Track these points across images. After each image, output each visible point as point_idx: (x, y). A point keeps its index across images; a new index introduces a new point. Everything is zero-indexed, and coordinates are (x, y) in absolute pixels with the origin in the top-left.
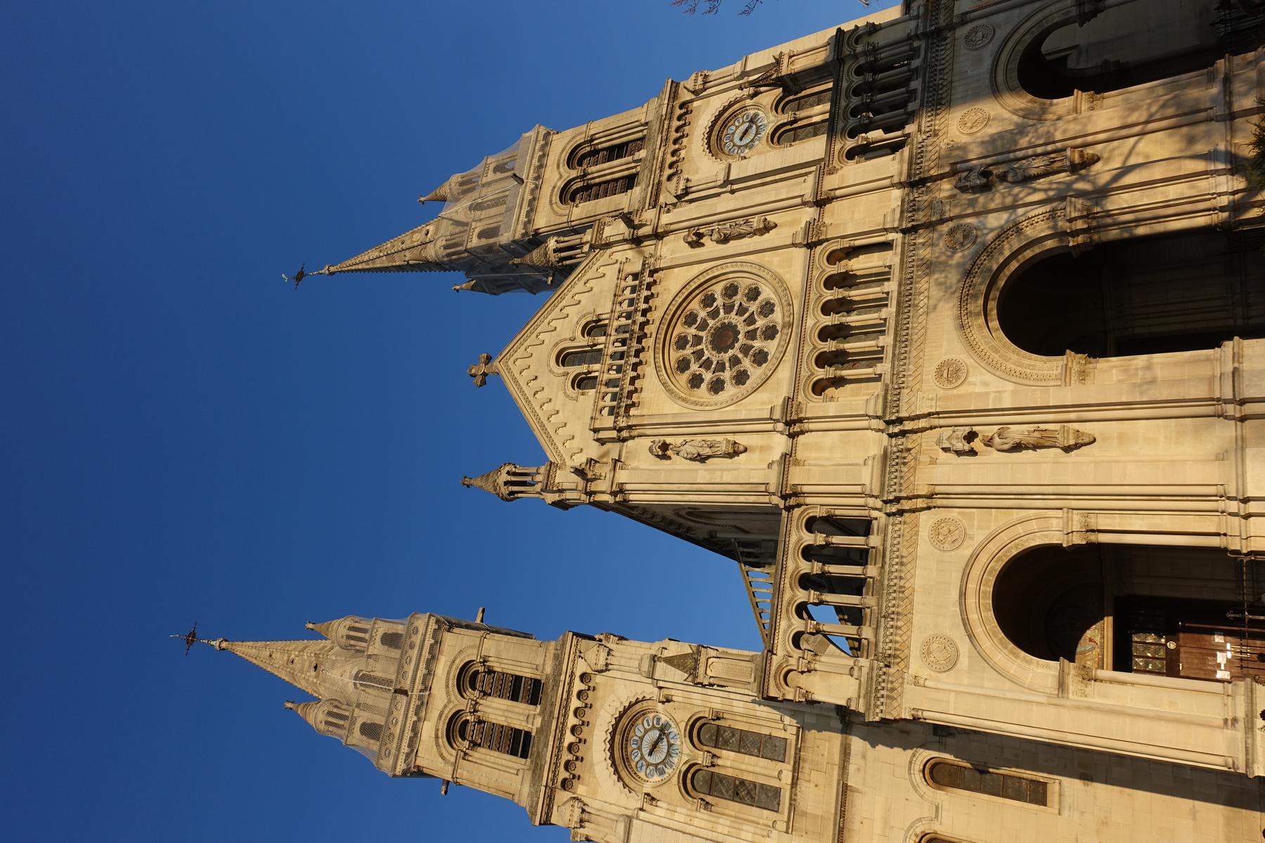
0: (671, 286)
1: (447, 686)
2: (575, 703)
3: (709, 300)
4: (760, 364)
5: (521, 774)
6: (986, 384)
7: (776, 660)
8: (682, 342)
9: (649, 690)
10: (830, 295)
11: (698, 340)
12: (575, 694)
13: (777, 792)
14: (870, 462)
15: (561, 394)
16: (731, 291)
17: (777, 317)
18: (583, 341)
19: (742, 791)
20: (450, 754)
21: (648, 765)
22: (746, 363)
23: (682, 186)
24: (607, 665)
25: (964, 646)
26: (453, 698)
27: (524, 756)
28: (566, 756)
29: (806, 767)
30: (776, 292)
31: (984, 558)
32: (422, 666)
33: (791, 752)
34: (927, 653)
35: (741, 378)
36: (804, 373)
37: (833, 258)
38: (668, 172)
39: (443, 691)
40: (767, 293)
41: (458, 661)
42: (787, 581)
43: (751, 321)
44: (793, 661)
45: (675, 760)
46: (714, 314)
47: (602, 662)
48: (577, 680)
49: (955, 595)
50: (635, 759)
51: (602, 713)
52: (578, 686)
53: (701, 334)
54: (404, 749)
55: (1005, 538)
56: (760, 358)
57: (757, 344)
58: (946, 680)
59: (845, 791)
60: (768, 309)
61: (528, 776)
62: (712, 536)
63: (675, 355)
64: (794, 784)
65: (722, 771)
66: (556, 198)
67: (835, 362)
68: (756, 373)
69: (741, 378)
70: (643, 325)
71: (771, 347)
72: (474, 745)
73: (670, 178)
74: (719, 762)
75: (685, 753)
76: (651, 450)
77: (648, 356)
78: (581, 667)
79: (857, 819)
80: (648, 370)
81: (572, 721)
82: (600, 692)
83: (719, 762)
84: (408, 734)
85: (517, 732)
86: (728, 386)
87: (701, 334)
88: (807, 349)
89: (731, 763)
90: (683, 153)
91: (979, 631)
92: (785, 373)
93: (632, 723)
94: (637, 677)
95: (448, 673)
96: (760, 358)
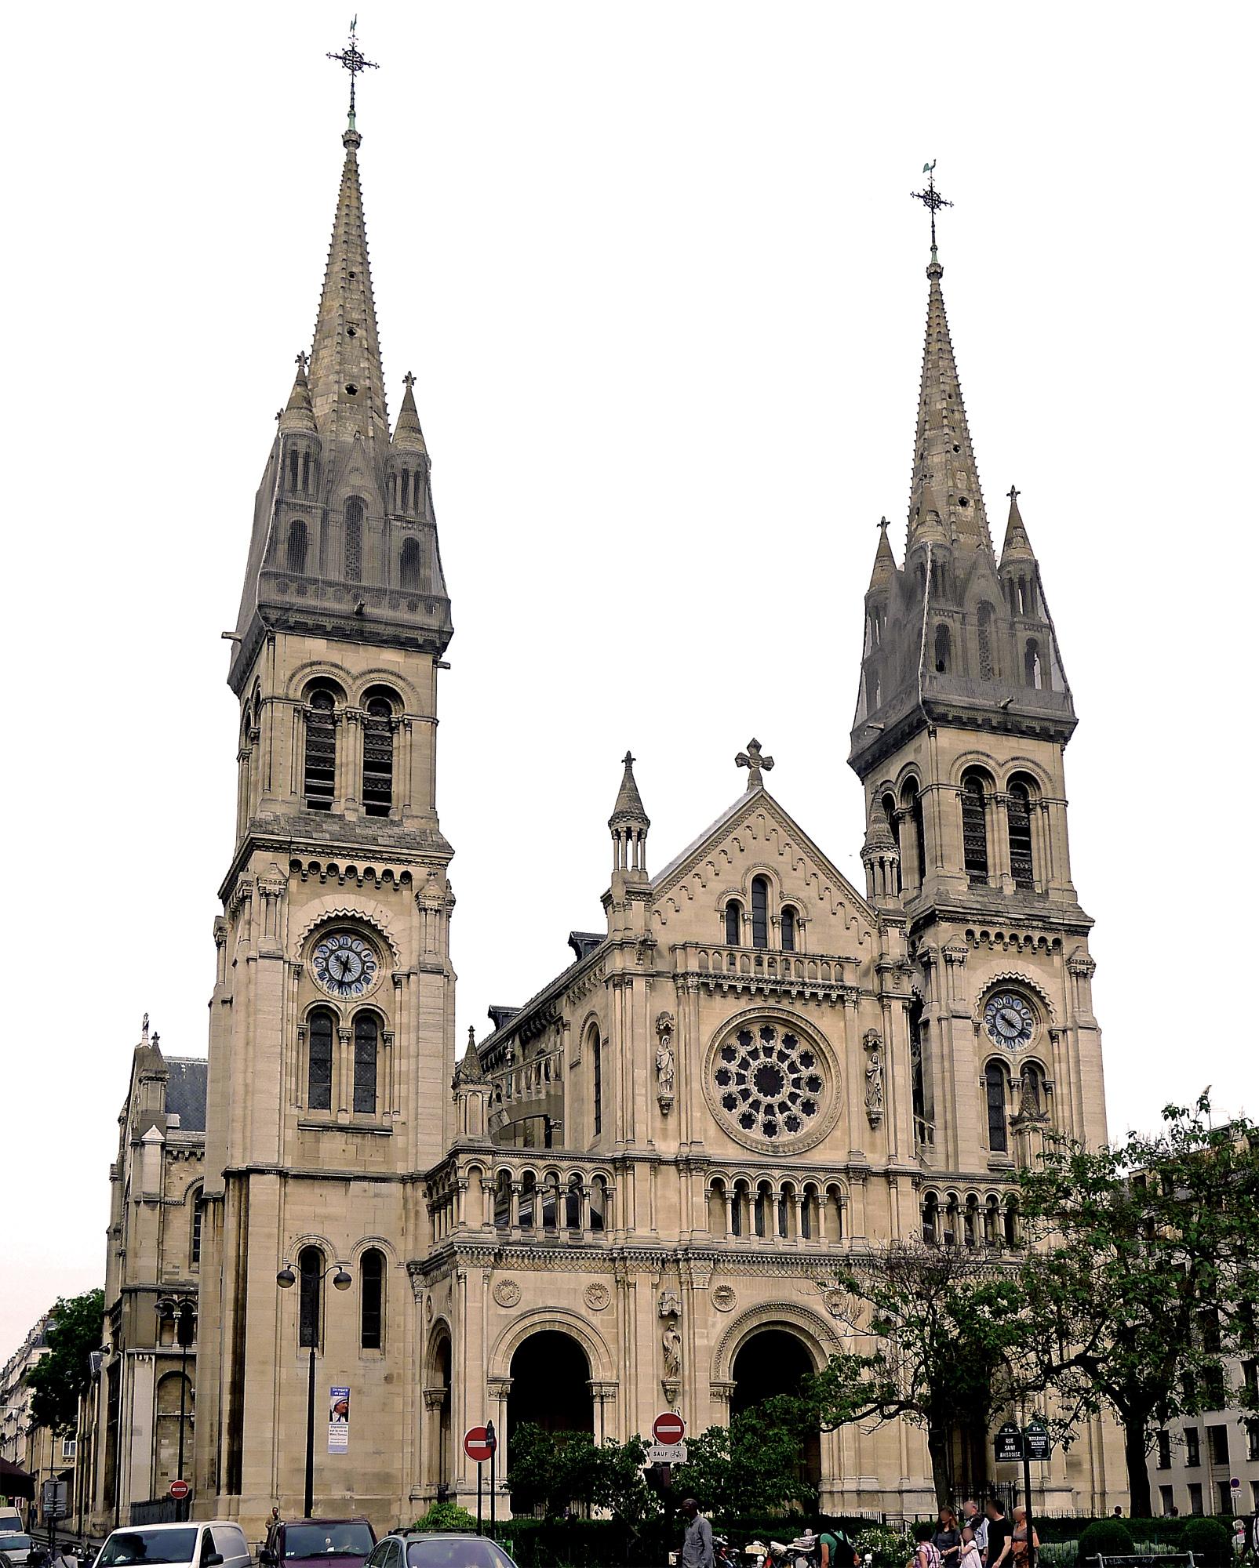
0: (824, 1021)
1: (371, 672)
2: (379, 868)
3: (807, 1060)
4: (741, 1121)
5: (292, 798)
6: (714, 1325)
7: (488, 1159)
8: (767, 1034)
9: (405, 962)
10: (799, 1189)
11: (768, 1051)
12: (390, 867)
13: (325, 1104)
14: (654, 1234)
15: (722, 887)
16: (814, 1083)
17: (785, 1136)
18: (775, 908)
19: (321, 1067)
20: (297, 691)
21: (326, 960)
22: (743, 1107)
23: (955, 955)
24: (425, 910)
25: (514, 1312)
26: (359, 682)
27: (309, 789)
28: (324, 861)
29: (358, 1140)
30: (808, 1135)
31: (580, 1324)
32: (390, 631)
33: (363, 1119)
34: (506, 1283)
35: (729, 1103)
36: (731, 1171)
37: (833, 1190)
38: (978, 930)
39: (363, 666)
40: (809, 1123)
41: (401, 682)
42: (552, 1162)
43: (783, 1107)
44: (489, 1174)
45: (336, 992)
46: (793, 1068)
47: (429, 904)
48: (403, 868)
49: (551, 1303)
50: (331, 944)
51: (373, 903)
52: (398, 870)
53: (775, 1055)
54: (293, 618)
55: (595, 1339)
56: (747, 1121)
57: (761, 1117)
58: (488, 1298)
59: (346, 1180)
60: (793, 1124)
61: (292, 811)
62: (564, 1026)
63: (756, 1030)
64: (342, 1129)
65: (335, 1047)
66: (972, 760)
67: (736, 1195)
68: (733, 1117)
69: (729, 1103)
70: (788, 992)
71: (756, 1133)
72: (307, 717)
73: (970, 933)
74: (344, 1045)
75: (347, 1005)
76: (664, 1014)
77: (759, 1003)
78: (418, 873)
79: (324, 1192)
80: (743, 1004)
81: (361, 866)
82: (393, 898)
83: (344, 1045)
84: (310, 621)
85: (330, 776)
86: (725, 1090)
87: (775, 1055)
88: (753, 1172)
89: (344, 1056)
90: (999, 947)
91: (527, 1322)
92: (732, 1153)
93: (364, 938)
94: (415, 945)
95: (385, 671)
96: (747, 1121)
